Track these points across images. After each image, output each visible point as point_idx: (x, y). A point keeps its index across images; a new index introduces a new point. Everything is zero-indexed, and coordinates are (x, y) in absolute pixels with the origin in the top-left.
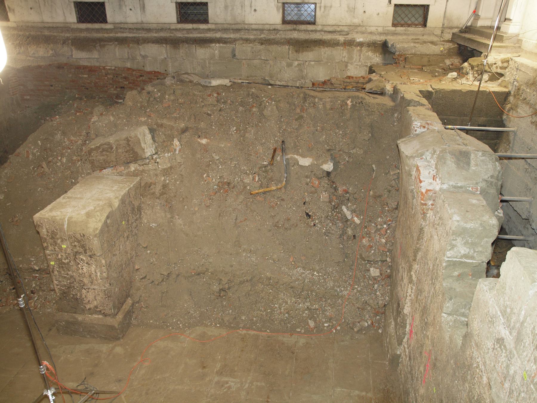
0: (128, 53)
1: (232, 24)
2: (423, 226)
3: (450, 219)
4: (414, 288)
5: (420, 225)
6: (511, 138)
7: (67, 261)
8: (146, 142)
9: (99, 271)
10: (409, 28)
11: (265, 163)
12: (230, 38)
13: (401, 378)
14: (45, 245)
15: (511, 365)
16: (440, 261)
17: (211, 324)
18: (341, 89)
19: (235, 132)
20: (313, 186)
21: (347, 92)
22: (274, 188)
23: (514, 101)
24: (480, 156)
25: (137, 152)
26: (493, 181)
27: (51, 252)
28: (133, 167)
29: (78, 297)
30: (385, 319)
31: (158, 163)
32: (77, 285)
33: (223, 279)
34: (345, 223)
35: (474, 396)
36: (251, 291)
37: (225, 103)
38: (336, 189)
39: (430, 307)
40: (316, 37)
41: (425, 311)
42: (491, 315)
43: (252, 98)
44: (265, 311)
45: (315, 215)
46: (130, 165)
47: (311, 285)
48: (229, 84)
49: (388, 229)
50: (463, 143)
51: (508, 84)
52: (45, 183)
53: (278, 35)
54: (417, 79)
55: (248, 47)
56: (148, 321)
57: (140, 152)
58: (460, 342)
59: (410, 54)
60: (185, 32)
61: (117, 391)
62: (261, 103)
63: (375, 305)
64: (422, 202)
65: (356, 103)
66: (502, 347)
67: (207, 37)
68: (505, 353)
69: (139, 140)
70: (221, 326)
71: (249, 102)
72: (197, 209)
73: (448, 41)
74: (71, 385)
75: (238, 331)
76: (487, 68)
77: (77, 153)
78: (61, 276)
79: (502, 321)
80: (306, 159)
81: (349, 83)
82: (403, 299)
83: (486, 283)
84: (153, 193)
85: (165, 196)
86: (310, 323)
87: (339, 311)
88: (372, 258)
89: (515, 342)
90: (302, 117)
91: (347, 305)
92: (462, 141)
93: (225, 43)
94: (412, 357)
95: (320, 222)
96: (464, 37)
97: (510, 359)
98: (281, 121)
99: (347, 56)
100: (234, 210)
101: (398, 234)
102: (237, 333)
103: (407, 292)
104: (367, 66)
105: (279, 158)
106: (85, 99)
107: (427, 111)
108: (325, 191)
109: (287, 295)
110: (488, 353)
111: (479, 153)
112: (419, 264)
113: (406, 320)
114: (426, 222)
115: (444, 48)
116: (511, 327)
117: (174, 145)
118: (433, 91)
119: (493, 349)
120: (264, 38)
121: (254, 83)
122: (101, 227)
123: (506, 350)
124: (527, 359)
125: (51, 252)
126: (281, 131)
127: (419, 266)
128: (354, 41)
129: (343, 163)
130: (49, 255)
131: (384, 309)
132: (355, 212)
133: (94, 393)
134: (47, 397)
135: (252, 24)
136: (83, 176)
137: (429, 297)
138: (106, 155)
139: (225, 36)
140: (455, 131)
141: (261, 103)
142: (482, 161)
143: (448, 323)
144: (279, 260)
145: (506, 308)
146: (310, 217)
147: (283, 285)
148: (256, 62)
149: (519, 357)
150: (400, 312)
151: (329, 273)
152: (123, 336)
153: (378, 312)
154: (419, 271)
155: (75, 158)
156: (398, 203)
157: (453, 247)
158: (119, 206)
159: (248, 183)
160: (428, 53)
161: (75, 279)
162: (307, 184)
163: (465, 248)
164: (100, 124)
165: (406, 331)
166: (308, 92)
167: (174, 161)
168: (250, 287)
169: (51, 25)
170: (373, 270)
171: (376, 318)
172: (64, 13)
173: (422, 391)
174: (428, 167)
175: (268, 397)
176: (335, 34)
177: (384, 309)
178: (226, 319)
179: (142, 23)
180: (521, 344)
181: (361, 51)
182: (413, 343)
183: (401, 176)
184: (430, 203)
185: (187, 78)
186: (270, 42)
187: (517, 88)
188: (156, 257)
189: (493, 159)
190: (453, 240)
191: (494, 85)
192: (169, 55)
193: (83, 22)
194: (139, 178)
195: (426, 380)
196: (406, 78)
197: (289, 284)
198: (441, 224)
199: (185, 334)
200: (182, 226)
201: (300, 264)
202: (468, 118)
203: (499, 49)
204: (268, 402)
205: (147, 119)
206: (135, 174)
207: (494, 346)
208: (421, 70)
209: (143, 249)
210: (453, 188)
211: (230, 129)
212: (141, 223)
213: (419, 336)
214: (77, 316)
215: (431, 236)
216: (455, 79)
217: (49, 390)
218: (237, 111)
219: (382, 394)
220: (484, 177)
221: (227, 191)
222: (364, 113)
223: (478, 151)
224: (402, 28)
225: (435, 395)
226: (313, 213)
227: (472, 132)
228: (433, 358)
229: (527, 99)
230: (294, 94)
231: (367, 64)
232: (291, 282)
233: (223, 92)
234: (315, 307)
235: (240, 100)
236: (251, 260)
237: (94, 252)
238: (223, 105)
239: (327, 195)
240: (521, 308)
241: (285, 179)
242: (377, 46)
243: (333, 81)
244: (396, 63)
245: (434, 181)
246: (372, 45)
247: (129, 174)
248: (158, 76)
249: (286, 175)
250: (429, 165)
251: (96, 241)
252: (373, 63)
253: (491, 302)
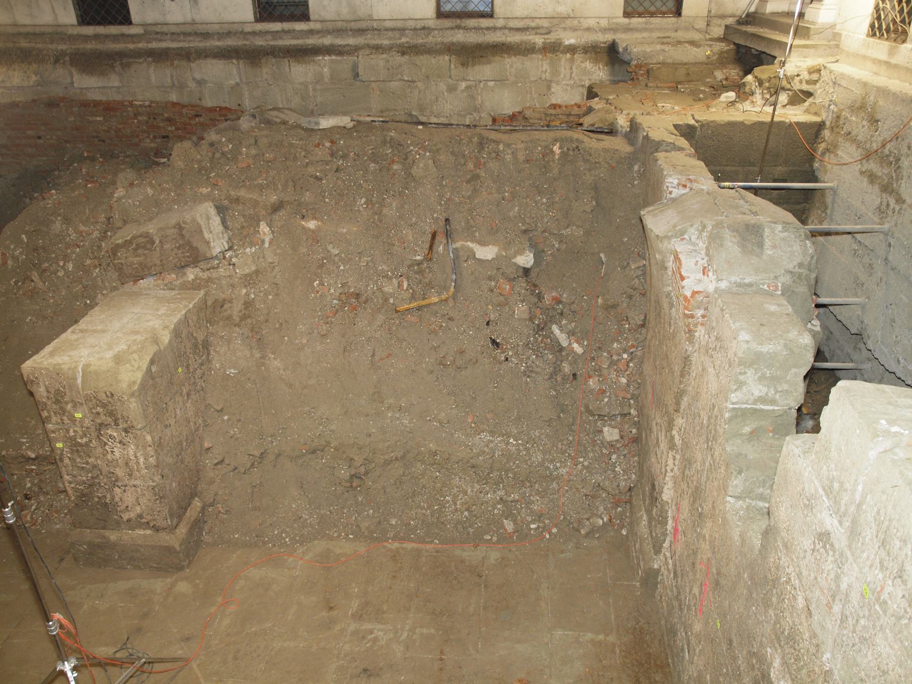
0: (172, 76)
1: (351, 21)
2: (689, 353)
3: (735, 338)
4: (678, 457)
5: (683, 351)
6: (829, 200)
7: (84, 440)
8: (212, 229)
9: (141, 455)
10: (652, 19)
11: (418, 258)
12: (348, 45)
13: (663, 607)
14: (45, 414)
15: (842, 575)
16: (720, 410)
17: (340, 535)
18: (543, 126)
19: (365, 206)
20: (500, 294)
21: (551, 132)
22: (435, 299)
23: (831, 138)
24: (779, 231)
25: (197, 248)
26: (802, 273)
27: (57, 426)
28: (191, 274)
29: (107, 501)
30: (631, 512)
31: (234, 265)
32: (105, 480)
33: (356, 459)
34: (558, 354)
35: (785, 630)
36: (403, 475)
37: (344, 157)
38: (540, 297)
39: (706, 487)
40: (496, 40)
41: (697, 494)
42: (807, 494)
43: (391, 147)
44: (429, 508)
45: (507, 343)
46: (185, 270)
47: (505, 461)
48: (351, 125)
49: (631, 360)
50: (750, 211)
51: (820, 109)
52: (38, 307)
53: (431, 38)
54: (668, 106)
55: (380, 61)
56: (232, 536)
57: (202, 247)
58: (757, 543)
59: (656, 64)
60: (269, 37)
61: (183, 656)
62: (406, 154)
63: (613, 489)
64: (686, 312)
65: (568, 149)
66: (828, 546)
67: (309, 45)
68: (833, 555)
69: (200, 227)
70: (356, 536)
71: (387, 155)
72: (304, 341)
73: (719, 40)
74: (103, 651)
75: (385, 544)
76: (784, 83)
77: (93, 253)
78: (76, 466)
79: (827, 502)
80: (487, 249)
81: (555, 115)
82: (661, 477)
83: (798, 442)
84: (229, 318)
85: (249, 321)
86: (506, 524)
87: (554, 503)
88: (606, 410)
89: (849, 538)
90: (477, 177)
91: (567, 491)
92: (749, 207)
94: (679, 572)
95: (516, 354)
96: (745, 31)
97: (840, 565)
98: (441, 185)
99: (549, 71)
100: (369, 340)
101: (647, 368)
102: (384, 547)
103: (667, 465)
104: (583, 86)
105: (441, 248)
106: (101, 160)
107: (688, 158)
108: (523, 301)
109: (465, 479)
110: (805, 557)
111: (777, 226)
112: (685, 416)
113: (667, 511)
114: (693, 346)
115: (711, 51)
116: (841, 513)
117: (261, 233)
118: (697, 125)
119: (813, 550)
120: (407, 43)
121: (393, 121)
122: (142, 380)
123: (834, 552)
124: (869, 563)
125: (57, 426)
126: (443, 202)
127: (684, 420)
128: (560, 44)
129: (550, 252)
130: (53, 432)
131: (628, 494)
132: (573, 335)
133: (145, 663)
134: (63, 673)
135: (385, 20)
136: (105, 292)
137: (703, 470)
138: (144, 255)
139: (339, 41)
140: (737, 191)
141: (406, 154)
142: (783, 239)
143: (737, 513)
144: (448, 422)
145: (832, 482)
146: (498, 347)
147: (457, 463)
148: (395, 85)
149: (855, 561)
150: (656, 498)
151: (534, 440)
152: (189, 564)
153: (619, 501)
154: (685, 429)
155: (88, 262)
156: (645, 317)
157: (741, 385)
158: (170, 341)
159: (390, 294)
160: (686, 61)
161: (100, 470)
162: (492, 291)
163: (761, 387)
164: (130, 201)
165: (666, 529)
166: (485, 133)
167: (261, 260)
168: (402, 469)
170: (608, 431)
171: (616, 512)
173: (697, 627)
174: (694, 254)
175: (442, 653)
176: (528, 33)
177: (628, 494)
178: (364, 525)
179: (194, 23)
180: (859, 540)
181: (572, 60)
182: (679, 549)
183: (648, 272)
184: (699, 313)
185: (277, 117)
186: (417, 50)
187: (834, 116)
188: (238, 426)
189: (800, 235)
190: (741, 374)
191: (797, 112)
192: (244, 80)
193: (89, 24)
194: (202, 292)
195: (704, 609)
196: (651, 104)
197: (468, 462)
198: (720, 348)
199: (295, 554)
200: (281, 371)
201: (486, 427)
202: (756, 169)
203: (804, 50)
204: (441, 659)
205: (212, 190)
206: (195, 286)
207: (815, 546)
208: (675, 89)
209: (216, 413)
210: (737, 286)
211: (356, 202)
212: (210, 369)
213: (689, 536)
214: (107, 533)
215: (703, 370)
216: (733, 103)
217: (66, 663)
218: (366, 171)
219: (632, 637)
220: (787, 267)
221: (355, 309)
222: (582, 166)
223: (775, 223)
224: (640, 20)
225: (720, 633)
226: (503, 338)
227: (764, 191)
228: (715, 571)
229: (853, 134)
230: (462, 137)
231: (583, 83)
232: (472, 458)
233: (340, 139)
234: (514, 497)
235: (370, 152)
236: (402, 423)
237: (131, 422)
238: (341, 162)
239: (525, 308)
240: (856, 480)
241: (453, 284)
242: (599, 52)
243: (528, 113)
244: (633, 79)
245: (706, 277)
246: (590, 50)
247: (185, 287)
248: (226, 115)
249: (454, 277)
250: (695, 251)
251: (134, 404)
252: (593, 81)
253: (806, 474)
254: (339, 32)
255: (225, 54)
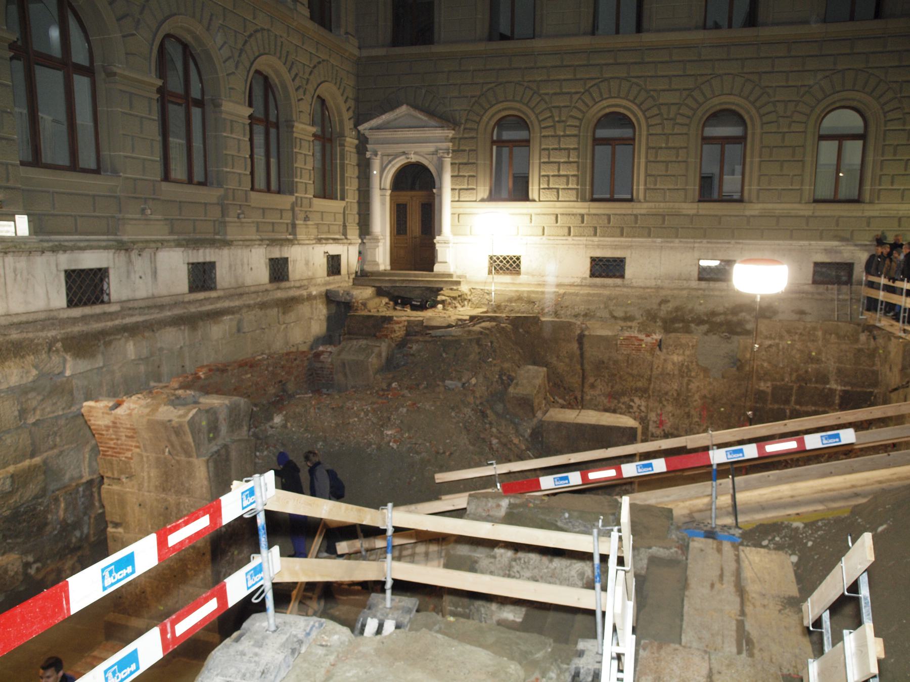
12: (236, 306)
60: (198, 304)
93: (233, 313)
139: (232, 304)
169: (24, 318)
172: (47, 292)
179: (153, 297)
193: (76, 305)
254: (230, 297)
255: (178, 321)
